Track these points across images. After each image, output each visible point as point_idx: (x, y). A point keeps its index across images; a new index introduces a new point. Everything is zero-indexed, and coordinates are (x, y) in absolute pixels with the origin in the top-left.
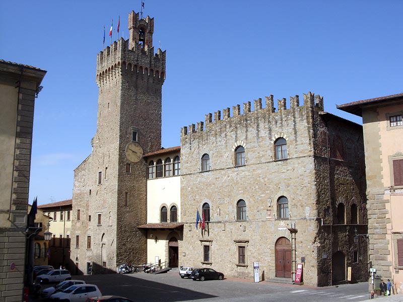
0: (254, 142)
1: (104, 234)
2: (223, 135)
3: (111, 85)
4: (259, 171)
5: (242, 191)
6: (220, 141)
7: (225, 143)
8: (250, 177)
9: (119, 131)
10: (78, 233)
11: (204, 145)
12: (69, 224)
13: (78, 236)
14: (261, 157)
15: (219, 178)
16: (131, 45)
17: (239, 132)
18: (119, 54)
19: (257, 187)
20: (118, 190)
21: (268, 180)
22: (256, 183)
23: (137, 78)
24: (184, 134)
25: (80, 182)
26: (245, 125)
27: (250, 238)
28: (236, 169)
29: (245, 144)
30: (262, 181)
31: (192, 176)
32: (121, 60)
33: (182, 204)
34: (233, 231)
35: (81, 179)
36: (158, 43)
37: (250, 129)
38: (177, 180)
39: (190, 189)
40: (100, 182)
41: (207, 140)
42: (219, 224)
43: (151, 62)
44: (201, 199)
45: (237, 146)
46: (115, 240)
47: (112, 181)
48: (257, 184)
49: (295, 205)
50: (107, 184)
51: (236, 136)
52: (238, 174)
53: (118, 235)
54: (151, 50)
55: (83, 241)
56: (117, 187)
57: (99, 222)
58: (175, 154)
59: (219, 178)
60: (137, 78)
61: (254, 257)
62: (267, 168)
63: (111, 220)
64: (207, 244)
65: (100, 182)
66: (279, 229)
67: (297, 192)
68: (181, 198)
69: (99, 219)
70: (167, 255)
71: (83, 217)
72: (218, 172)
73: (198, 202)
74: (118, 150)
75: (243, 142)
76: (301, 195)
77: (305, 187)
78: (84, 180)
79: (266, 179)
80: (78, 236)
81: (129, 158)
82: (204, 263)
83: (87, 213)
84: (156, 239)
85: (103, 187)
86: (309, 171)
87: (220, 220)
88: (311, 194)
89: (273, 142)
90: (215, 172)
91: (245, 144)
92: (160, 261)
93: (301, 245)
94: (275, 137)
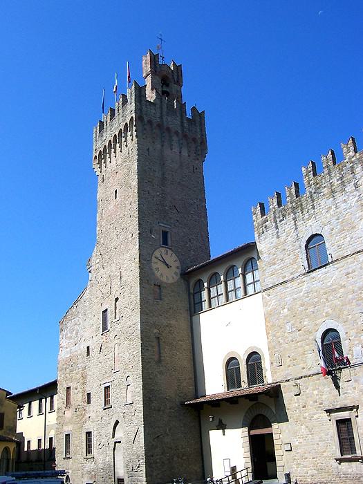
1: (117, 422)
2: (350, 187)
3: (119, 162)
9: (137, 227)
10: (67, 429)
11: (308, 219)
12: (52, 418)
13: (68, 436)
15: (354, 271)
16: (150, 95)
18: (131, 106)
23: (162, 146)
31: (289, 285)
33: (274, 344)
35: (72, 333)
36: (192, 95)
39: (286, 310)
41: (313, 208)
43: (182, 122)
44: (316, 325)
46: (142, 429)
47: (130, 320)
54: (182, 106)
55: (78, 442)
57: (107, 402)
58: (246, 255)
59: (354, 271)
60: (162, 146)
63: (131, 393)
64: (344, 415)
65: (105, 328)
68: (268, 333)
69: (107, 396)
70: (249, 454)
71: (77, 398)
72: (350, 260)
74: (137, 260)
80: (68, 436)
81: (158, 274)
84: (222, 426)
85: (112, 335)
90: (342, 263)
92: (233, 469)
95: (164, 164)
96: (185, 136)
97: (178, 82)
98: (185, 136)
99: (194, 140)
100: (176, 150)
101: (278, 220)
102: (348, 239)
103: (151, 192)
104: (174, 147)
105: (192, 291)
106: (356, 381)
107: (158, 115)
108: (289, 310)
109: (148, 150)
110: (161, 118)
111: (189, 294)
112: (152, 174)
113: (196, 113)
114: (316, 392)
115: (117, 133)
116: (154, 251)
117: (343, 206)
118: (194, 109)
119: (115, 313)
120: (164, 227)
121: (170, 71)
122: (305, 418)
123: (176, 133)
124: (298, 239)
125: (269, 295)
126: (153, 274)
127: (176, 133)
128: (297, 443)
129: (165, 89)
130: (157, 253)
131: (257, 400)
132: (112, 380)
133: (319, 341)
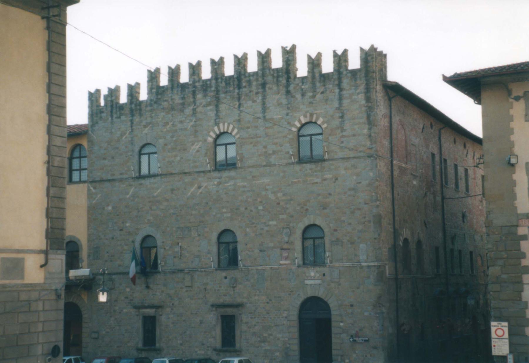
0: (256, 127)
2: (188, 111)
4: (266, 180)
5: (229, 215)
6: (181, 122)
7: (192, 126)
8: (246, 189)
11: (145, 127)
14: (270, 154)
17: (222, 107)
19: (260, 208)
21: (284, 195)
22: (259, 200)
26: (236, 96)
27: (245, 300)
28: (216, 174)
29: (236, 131)
30: (272, 197)
31: (117, 184)
34: (209, 287)
37: (247, 104)
39: (110, 208)
42: (180, 275)
45: (218, 133)
48: (261, 202)
49: (338, 240)
51: (217, 116)
52: (219, 183)
61: (254, 334)
62: (282, 174)
66: (307, 282)
67: (343, 218)
73: (129, 233)
75: (231, 127)
76: (350, 224)
77: (359, 209)
79: (280, 195)
82: (142, 350)
86: (367, 182)
87: (182, 266)
88: (369, 221)
89: (294, 129)
91: (236, 131)
93: (350, 311)
94: (300, 121)
101: (115, 116)
102: (178, 158)
106: (165, 285)
108: (113, 208)
114: (128, 290)
117: (179, 126)
122: (114, 311)
124: (132, 142)
125: (95, 188)
128: (104, 332)
133: (137, 245)
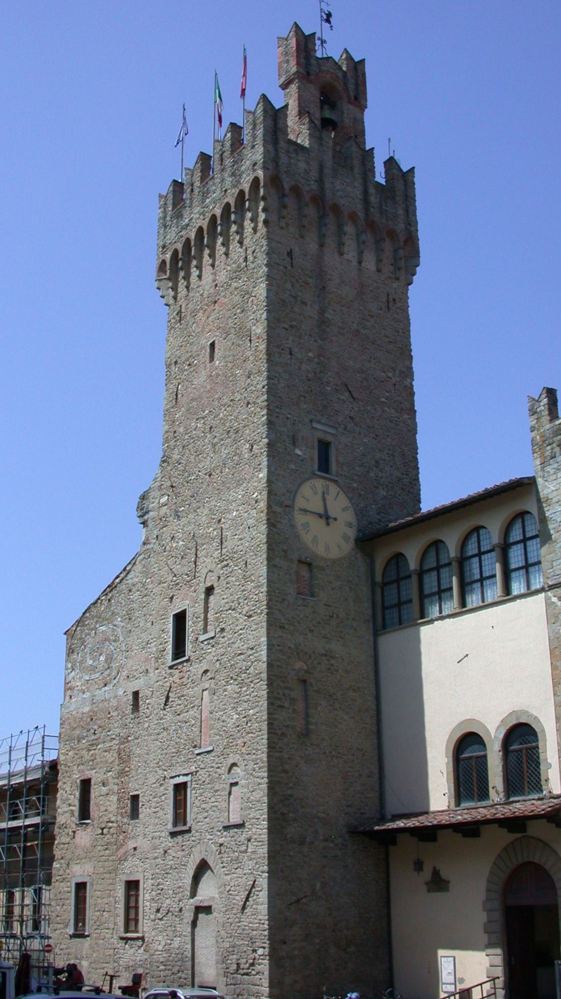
3: (222, 277)
9: (263, 430)
13: (81, 887)
20: (270, 665)
23: (322, 245)
24: (546, 418)
25: (93, 669)
32: (265, 168)
38: (536, 604)
40: (179, 649)
43: (366, 193)
46: (263, 882)
50: (212, 653)
53: (273, 856)
56: (264, 653)
60: (322, 245)
74: (263, 505)
78: (110, 659)
80: (81, 887)
81: (307, 538)
83: (123, 786)
85: (196, 669)
95: (324, 287)
96: (371, 225)
97: (356, 98)
98: (371, 225)
99: (392, 234)
100: (351, 254)
103: (295, 350)
104: (346, 249)
105: (378, 578)
107: (314, 174)
109: (290, 254)
110: (320, 181)
111: (373, 584)
112: (296, 309)
113: (395, 171)
115: (218, 212)
116: (299, 486)
118: (391, 163)
119: (206, 619)
120: (322, 430)
121: (340, 75)
123: (353, 217)
126: (297, 537)
127: (353, 217)
129: (328, 114)
130: (306, 489)
131: (525, 831)
132: (193, 769)
